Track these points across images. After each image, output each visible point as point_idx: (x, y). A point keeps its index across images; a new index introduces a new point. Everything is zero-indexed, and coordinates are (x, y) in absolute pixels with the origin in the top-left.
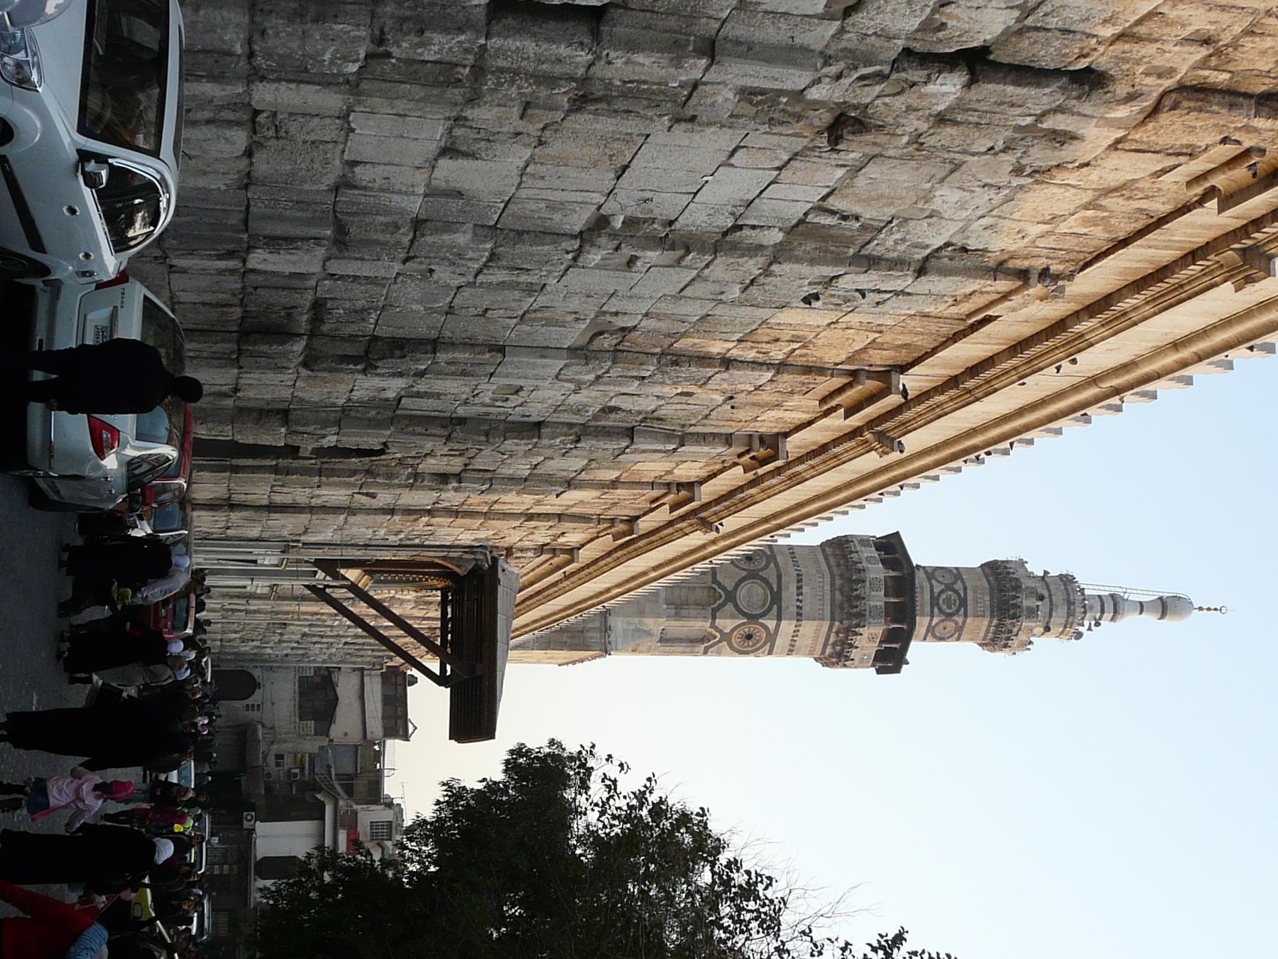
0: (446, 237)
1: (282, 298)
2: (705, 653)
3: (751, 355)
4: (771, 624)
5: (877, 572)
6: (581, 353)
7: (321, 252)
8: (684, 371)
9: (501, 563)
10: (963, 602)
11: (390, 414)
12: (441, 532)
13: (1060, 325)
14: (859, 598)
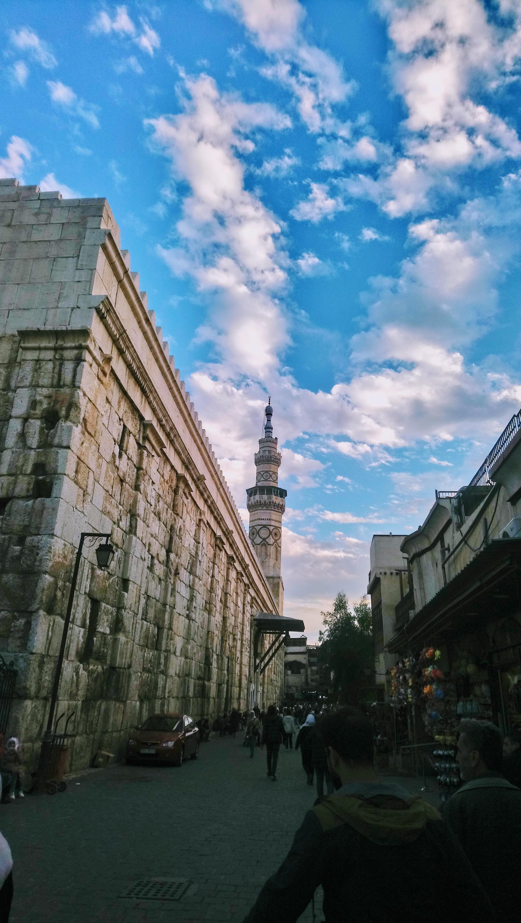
0: (189, 651)
1: (197, 688)
2: (280, 547)
3: (211, 571)
4: (272, 528)
5: (257, 497)
6: (210, 612)
7: (190, 679)
8: (214, 587)
9: (255, 618)
10: (267, 472)
11: (220, 657)
12: (247, 637)
13: (209, 507)
14: (265, 502)
